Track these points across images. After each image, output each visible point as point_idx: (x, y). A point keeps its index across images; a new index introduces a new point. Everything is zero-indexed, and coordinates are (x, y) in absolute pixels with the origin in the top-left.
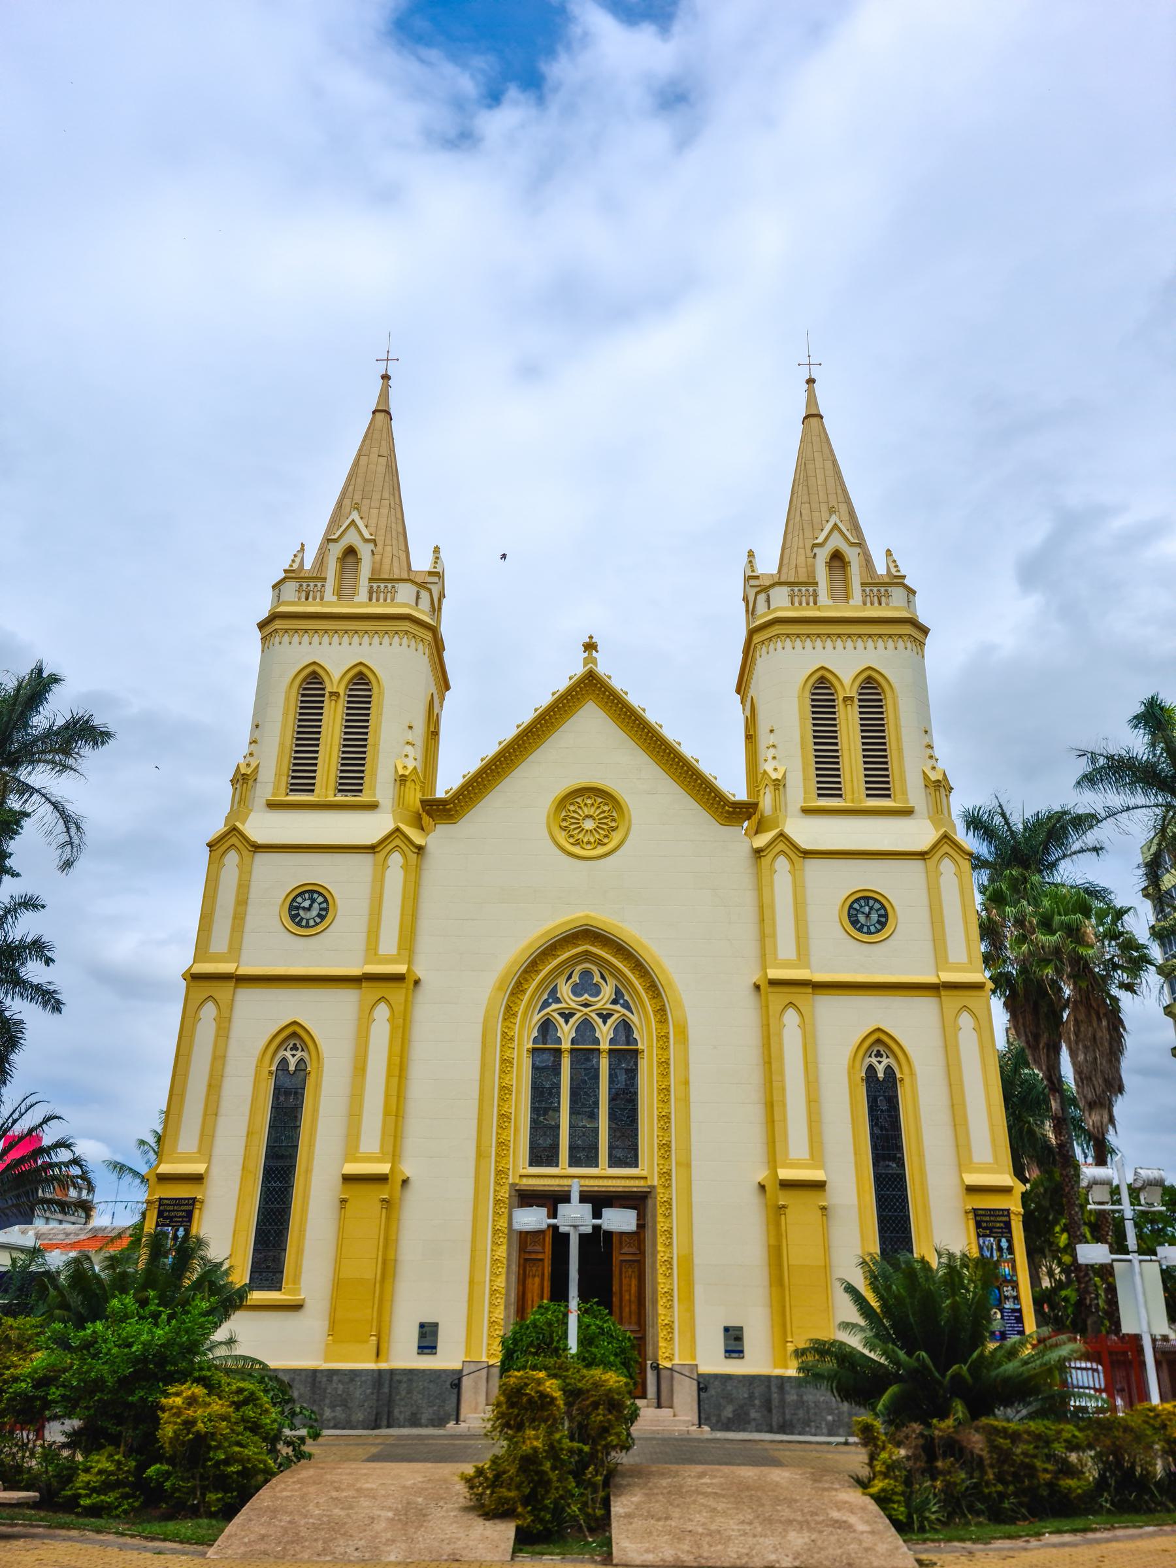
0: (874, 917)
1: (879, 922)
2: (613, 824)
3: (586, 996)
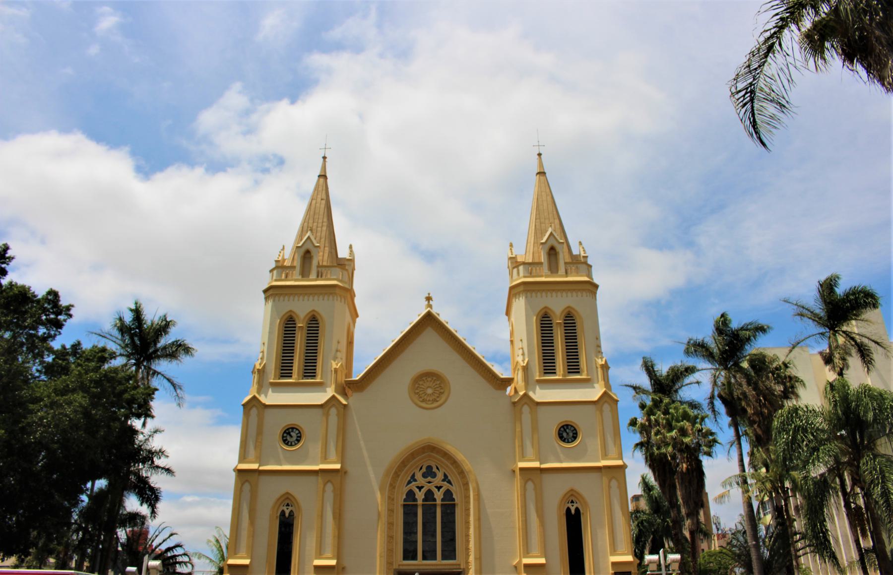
0: (571, 434)
1: (573, 437)
3: (429, 478)
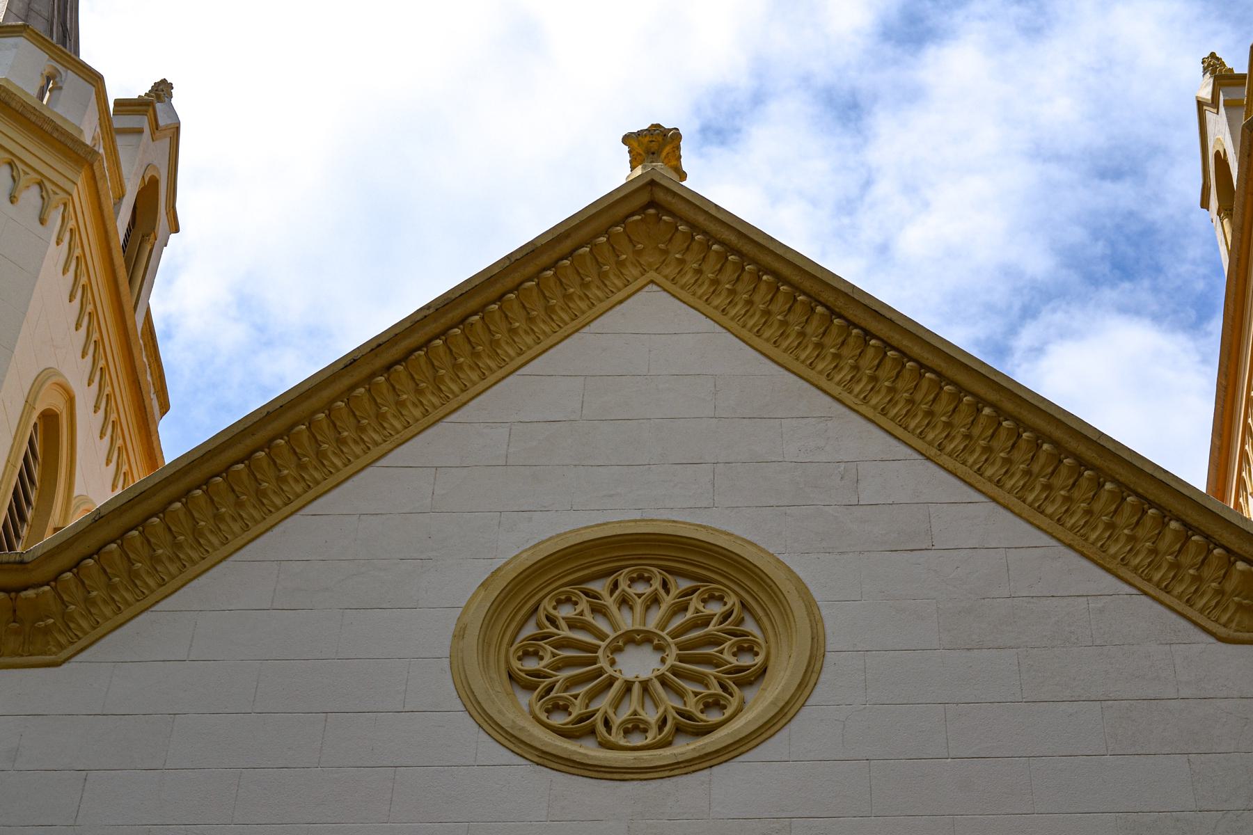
2: (746, 660)
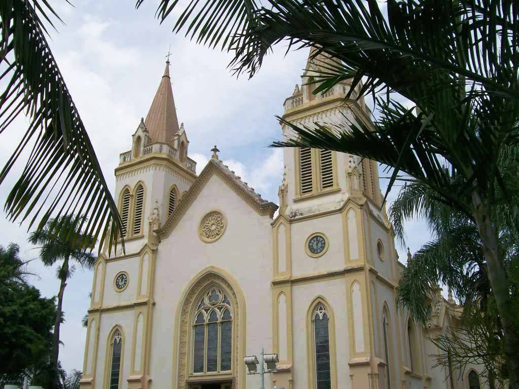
0: (320, 245)
